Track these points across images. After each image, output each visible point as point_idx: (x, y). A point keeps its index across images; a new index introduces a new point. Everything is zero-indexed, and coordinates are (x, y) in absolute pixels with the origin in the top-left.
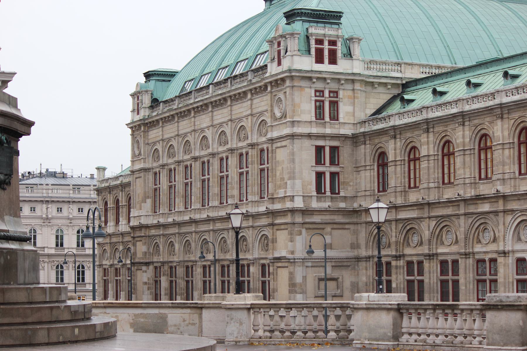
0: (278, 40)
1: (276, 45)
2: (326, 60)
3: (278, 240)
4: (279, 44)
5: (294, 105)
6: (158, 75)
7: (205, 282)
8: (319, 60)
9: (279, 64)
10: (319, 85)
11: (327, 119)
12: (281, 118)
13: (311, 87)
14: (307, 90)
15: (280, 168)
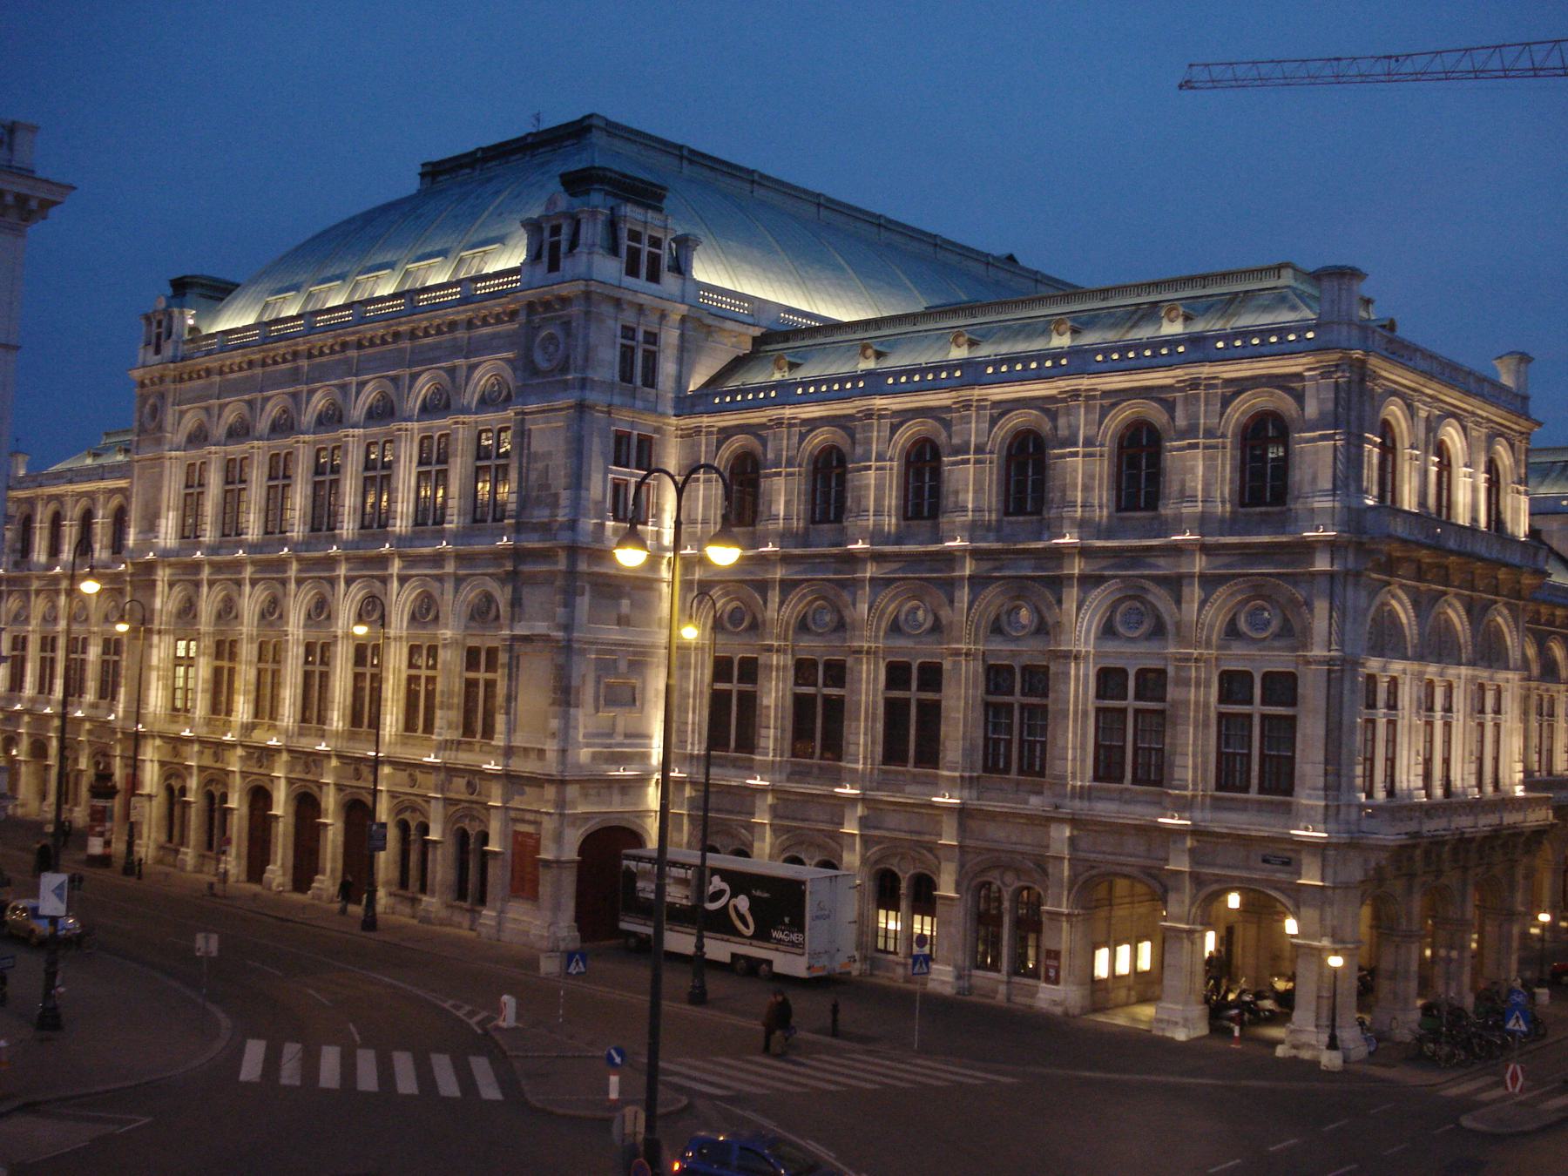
0: (554, 222)
1: (547, 233)
2: (643, 271)
3: (525, 601)
4: (556, 230)
5: (587, 348)
6: (202, 285)
7: (307, 676)
8: (632, 270)
9: (554, 266)
10: (629, 317)
11: (639, 381)
12: (552, 370)
13: (616, 319)
14: (610, 323)
15: (540, 465)
